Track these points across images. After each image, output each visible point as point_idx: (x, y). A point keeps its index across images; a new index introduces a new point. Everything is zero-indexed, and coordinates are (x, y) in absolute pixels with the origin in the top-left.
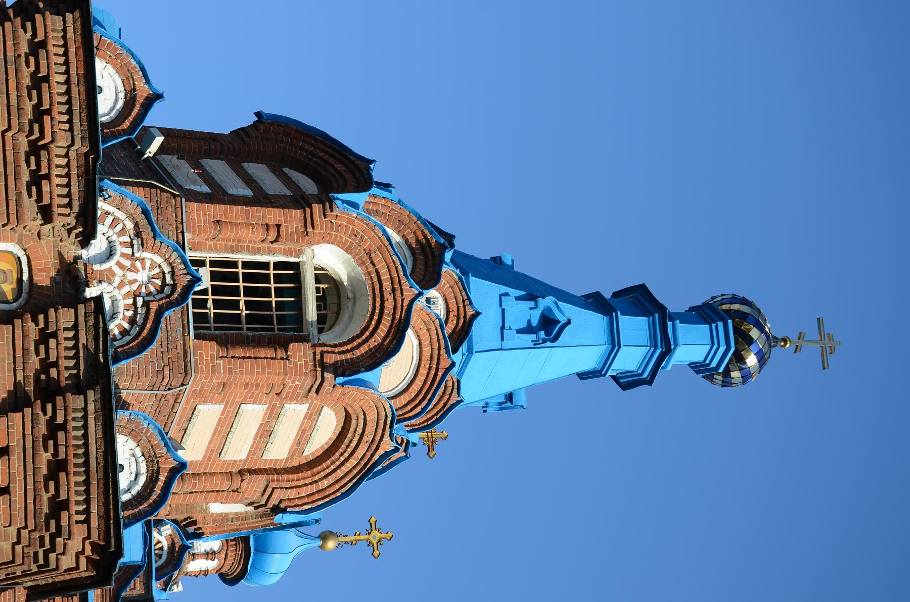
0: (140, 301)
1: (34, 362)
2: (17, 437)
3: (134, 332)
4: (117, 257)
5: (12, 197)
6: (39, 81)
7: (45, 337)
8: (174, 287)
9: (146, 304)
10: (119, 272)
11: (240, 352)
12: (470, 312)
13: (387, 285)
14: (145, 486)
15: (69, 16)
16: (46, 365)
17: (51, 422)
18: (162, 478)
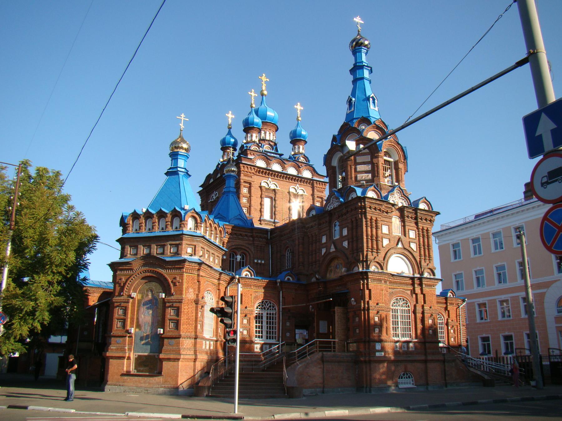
0: (401, 198)
1: (410, 219)
2: (421, 225)
3: (405, 200)
4: (394, 200)
5: (389, 217)
6: (375, 209)
7: (408, 217)
8: (399, 191)
9: (402, 197)
10: (397, 200)
11: (400, 178)
12: (380, 120)
13: (390, 143)
14: (426, 204)
15: (366, 200)
16: (412, 218)
17: (420, 219)
18: (426, 201)
